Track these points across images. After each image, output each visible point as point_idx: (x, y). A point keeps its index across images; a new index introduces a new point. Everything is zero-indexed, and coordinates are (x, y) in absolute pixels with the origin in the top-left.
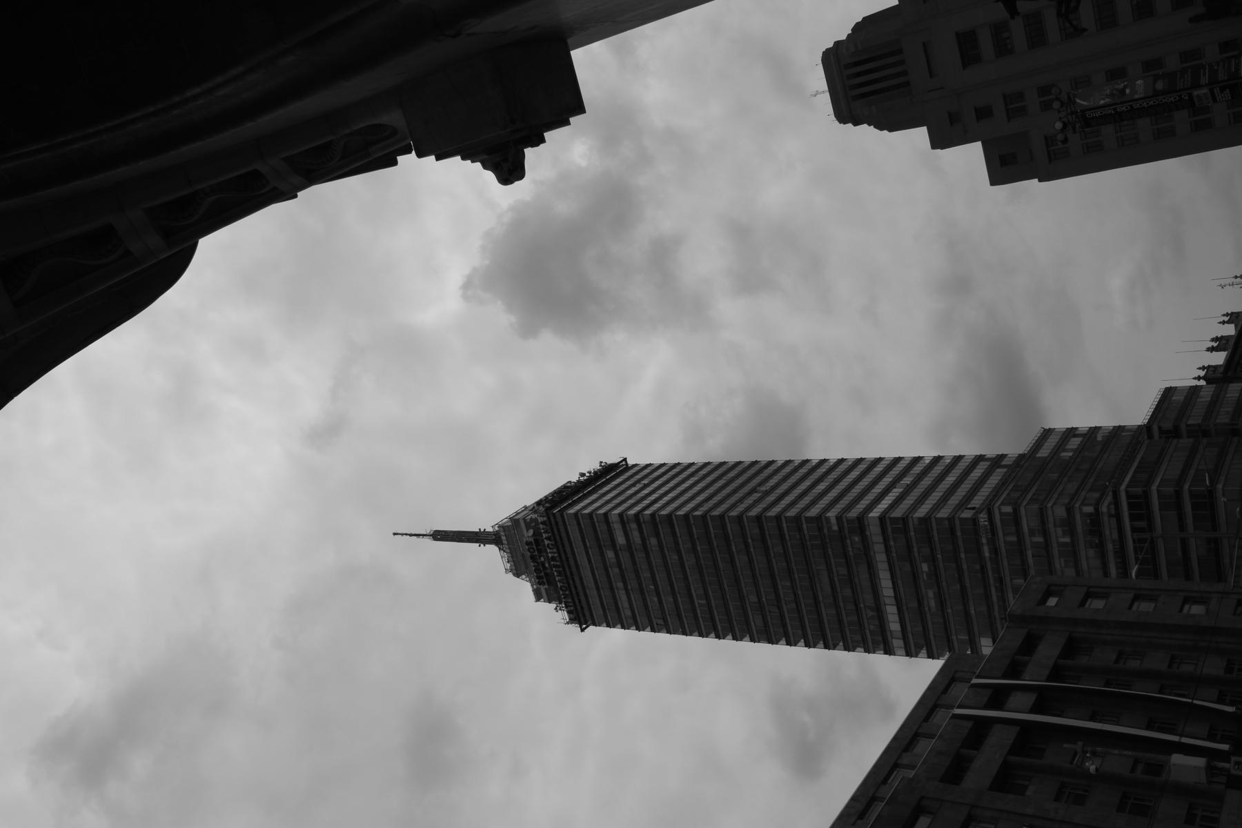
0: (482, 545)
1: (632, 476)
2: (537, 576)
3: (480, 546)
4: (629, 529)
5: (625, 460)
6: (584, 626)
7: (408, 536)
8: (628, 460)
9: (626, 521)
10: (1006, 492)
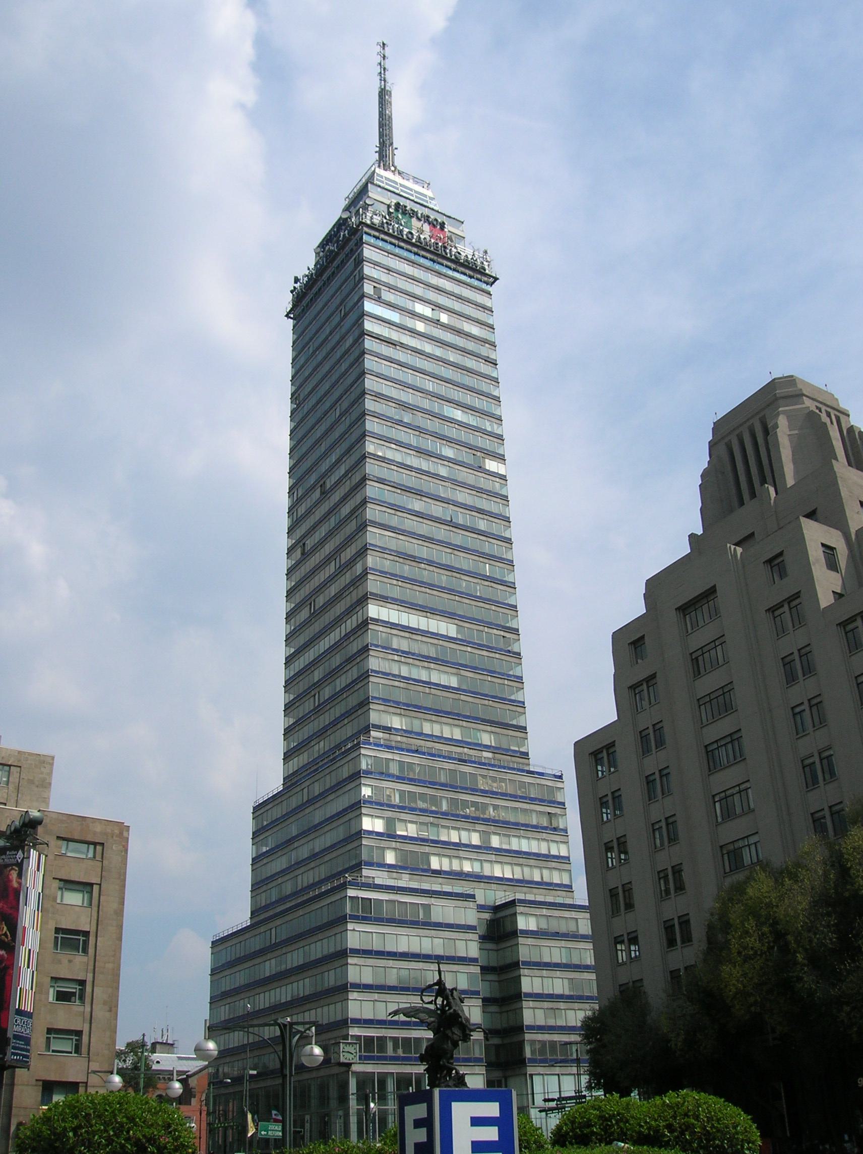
0: (377, 154)
1: (459, 298)
2: (328, 239)
3: (376, 152)
4: (354, 329)
5: (496, 279)
6: (292, 316)
7: (379, 59)
8: (498, 281)
9: (359, 322)
10: (397, 758)
